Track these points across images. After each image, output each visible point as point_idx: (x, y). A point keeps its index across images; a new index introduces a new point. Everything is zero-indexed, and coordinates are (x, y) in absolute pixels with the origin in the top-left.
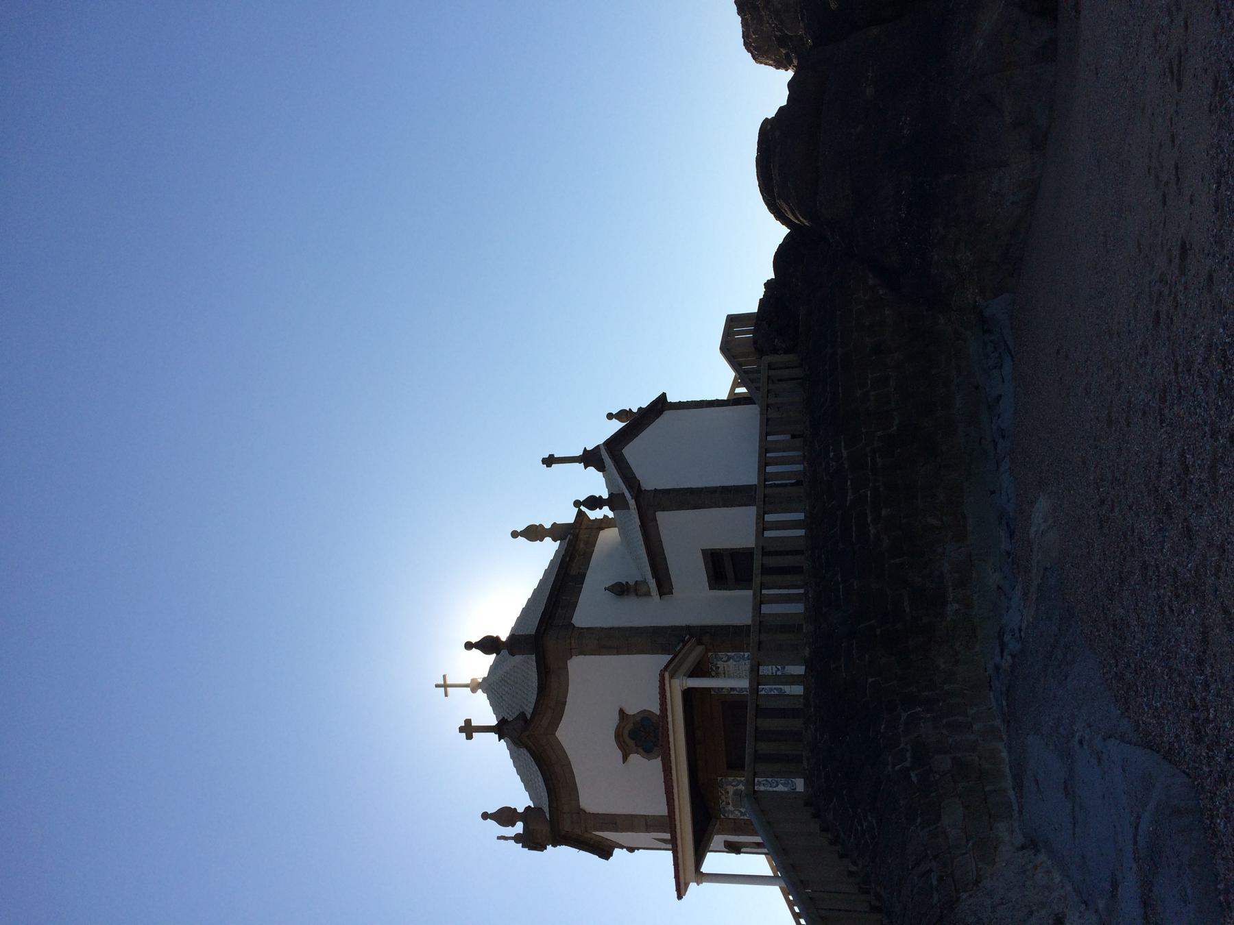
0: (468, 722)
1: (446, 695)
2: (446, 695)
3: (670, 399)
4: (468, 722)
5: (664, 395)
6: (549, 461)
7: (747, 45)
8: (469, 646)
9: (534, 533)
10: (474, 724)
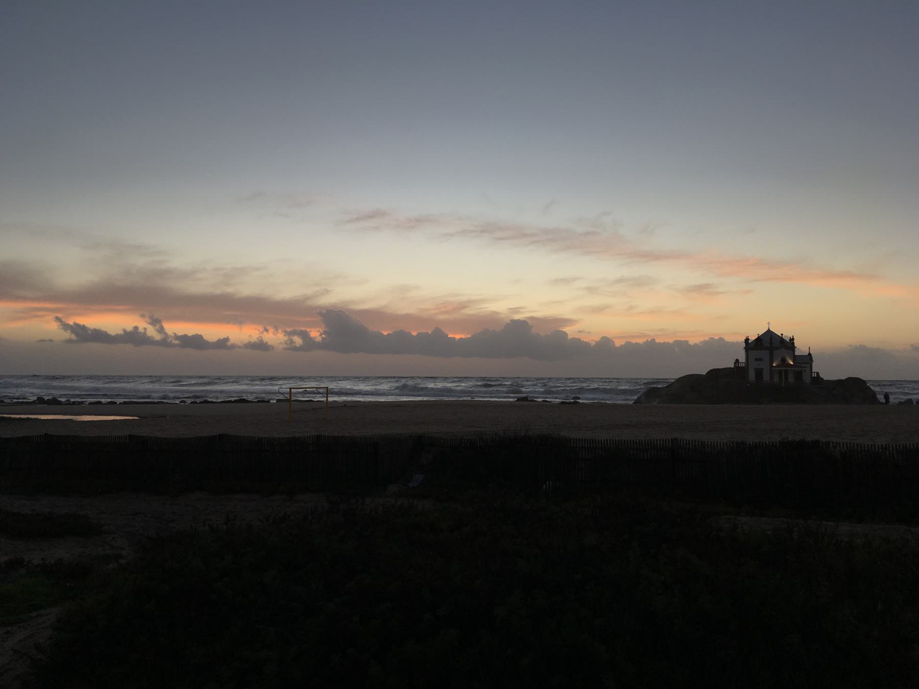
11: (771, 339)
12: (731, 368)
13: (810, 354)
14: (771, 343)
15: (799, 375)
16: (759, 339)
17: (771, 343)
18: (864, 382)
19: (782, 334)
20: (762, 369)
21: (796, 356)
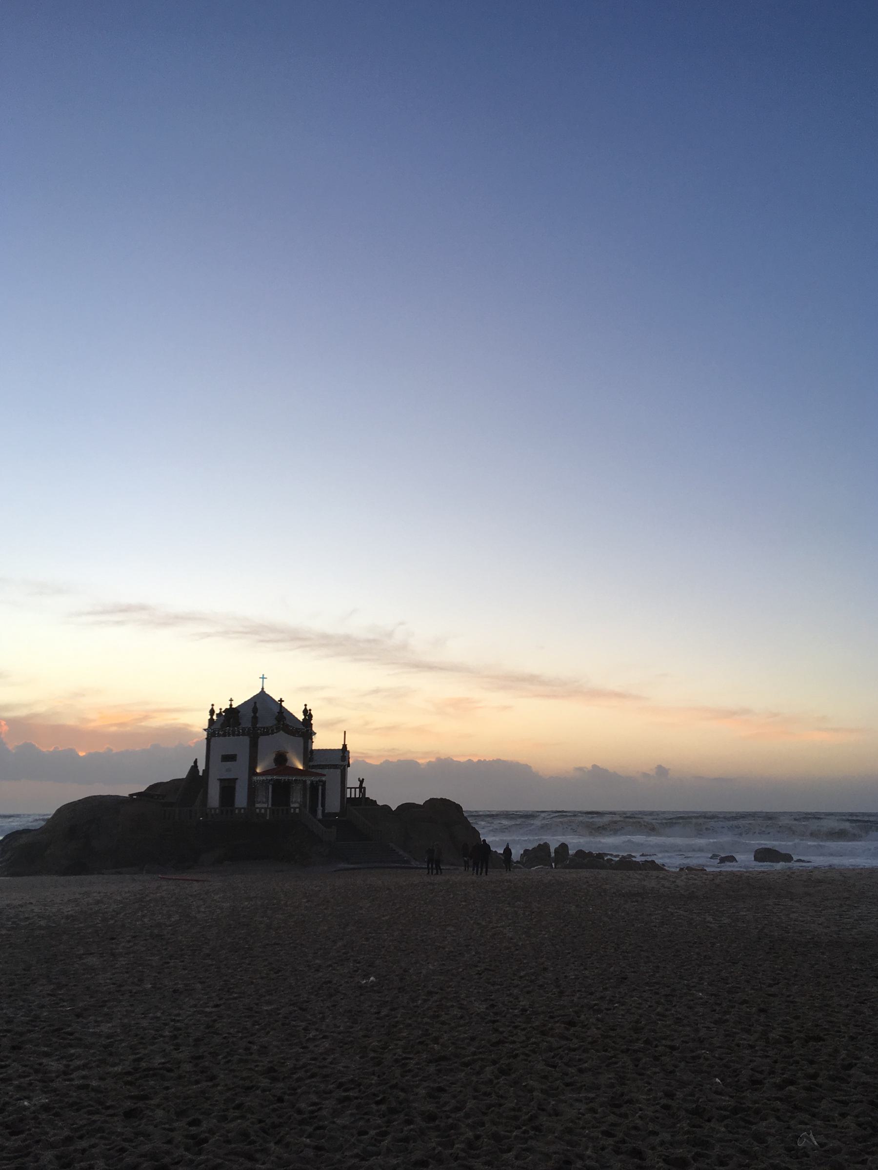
0: (283, 701)
1: (260, 678)
2: (260, 678)
3: (348, 768)
4: (283, 701)
5: (349, 766)
7: (431, 799)
9: (311, 716)
11: (255, 710)
12: (183, 779)
13: (345, 746)
14: (255, 719)
15: (316, 791)
16: (231, 713)
17: (255, 719)
18: (458, 808)
19: (281, 701)
20: (234, 780)
21: (312, 751)
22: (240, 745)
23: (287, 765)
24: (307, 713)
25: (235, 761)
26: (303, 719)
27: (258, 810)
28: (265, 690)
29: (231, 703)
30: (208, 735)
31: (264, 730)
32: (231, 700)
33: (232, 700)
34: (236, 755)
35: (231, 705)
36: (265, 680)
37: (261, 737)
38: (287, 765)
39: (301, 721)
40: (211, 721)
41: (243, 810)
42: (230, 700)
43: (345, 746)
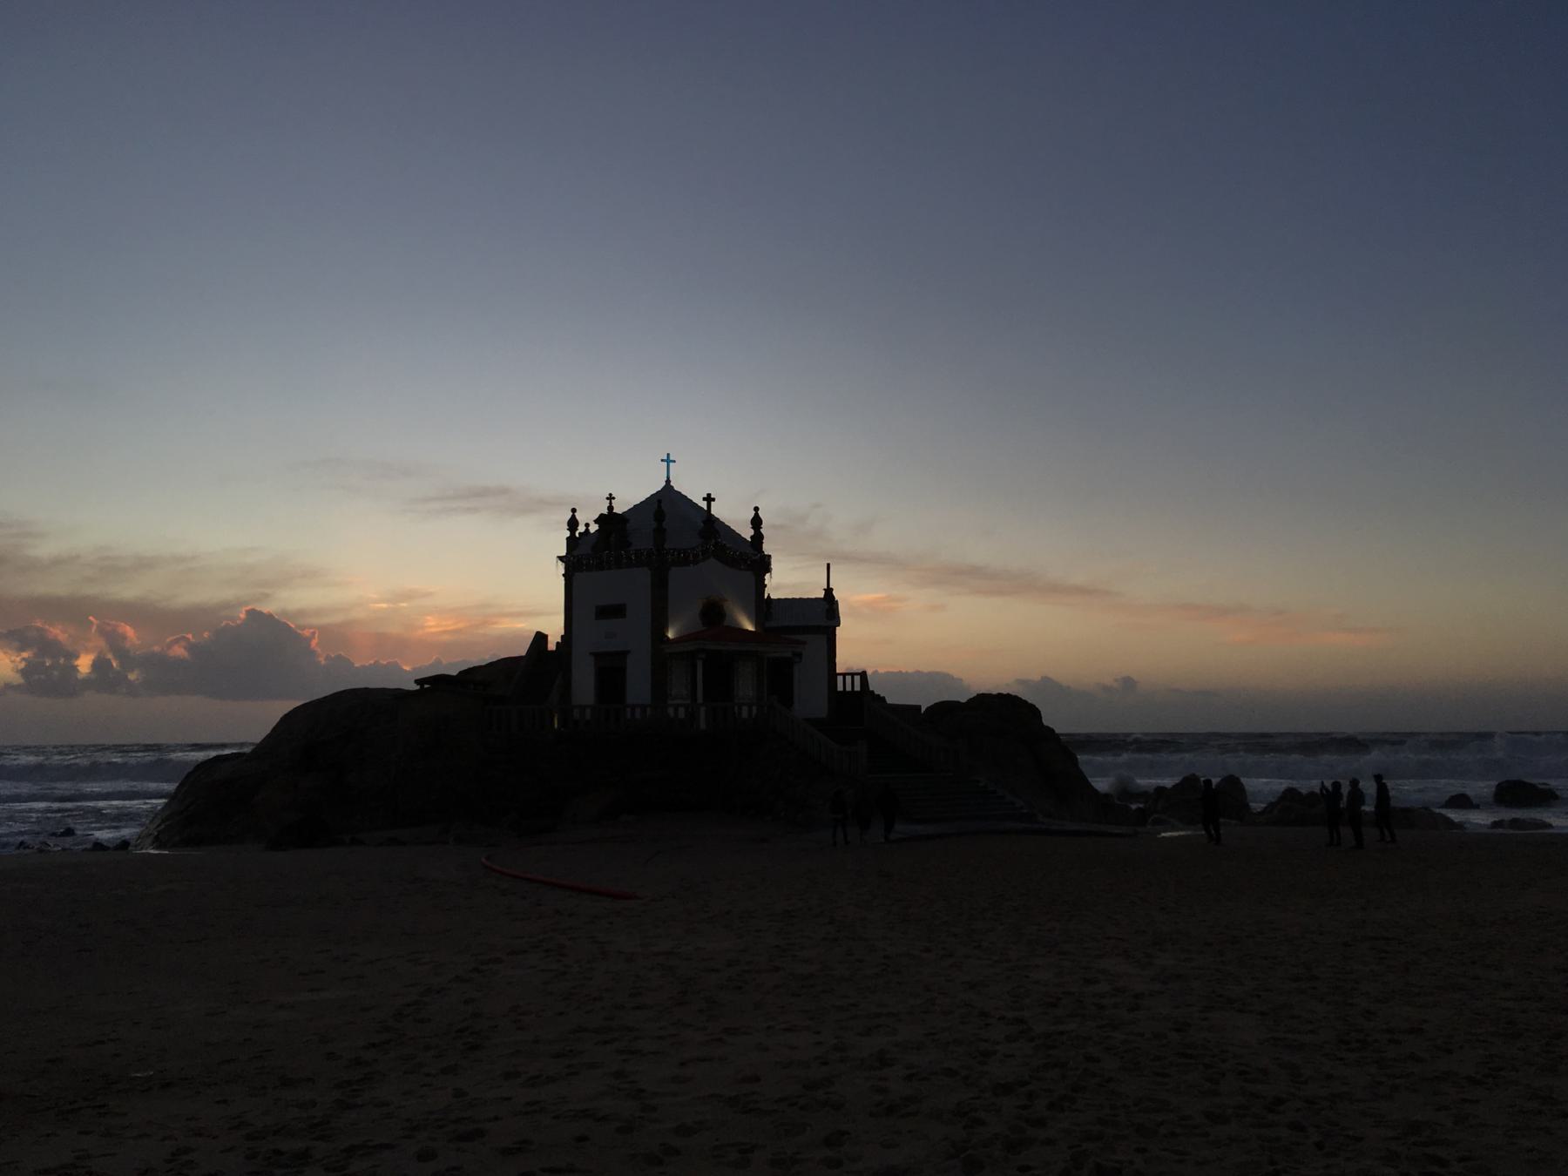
0: (714, 500)
1: (662, 460)
2: (662, 460)
4: (714, 500)
6: (828, 565)
8: (756, 509)
10: (712, 503)
11: (659, 515)
12: (521, 657)
13: (829, 591)
14: (660, 532)
15: (779, 678)
16: (609, 520)
17: (660, 532)
22: (633, 585)
23: (726, 624)
24: (756, 522)
25: (624, 616)
26: (752, 537)
27: (671, 711)
28: (672, 484)
29: (611, 503)
30: (566, 569)
31: (679, 554)
32: (611, 498)
33: (614, 498)
34: (625, 605)
35: (610, 508)
36: (671, 464)
37: (674, 569)
38: (726, 624)
39: (750, 540)
40: (572, 542)
41: (638, 711)
42: (607, 498)
43: (829, 591)
